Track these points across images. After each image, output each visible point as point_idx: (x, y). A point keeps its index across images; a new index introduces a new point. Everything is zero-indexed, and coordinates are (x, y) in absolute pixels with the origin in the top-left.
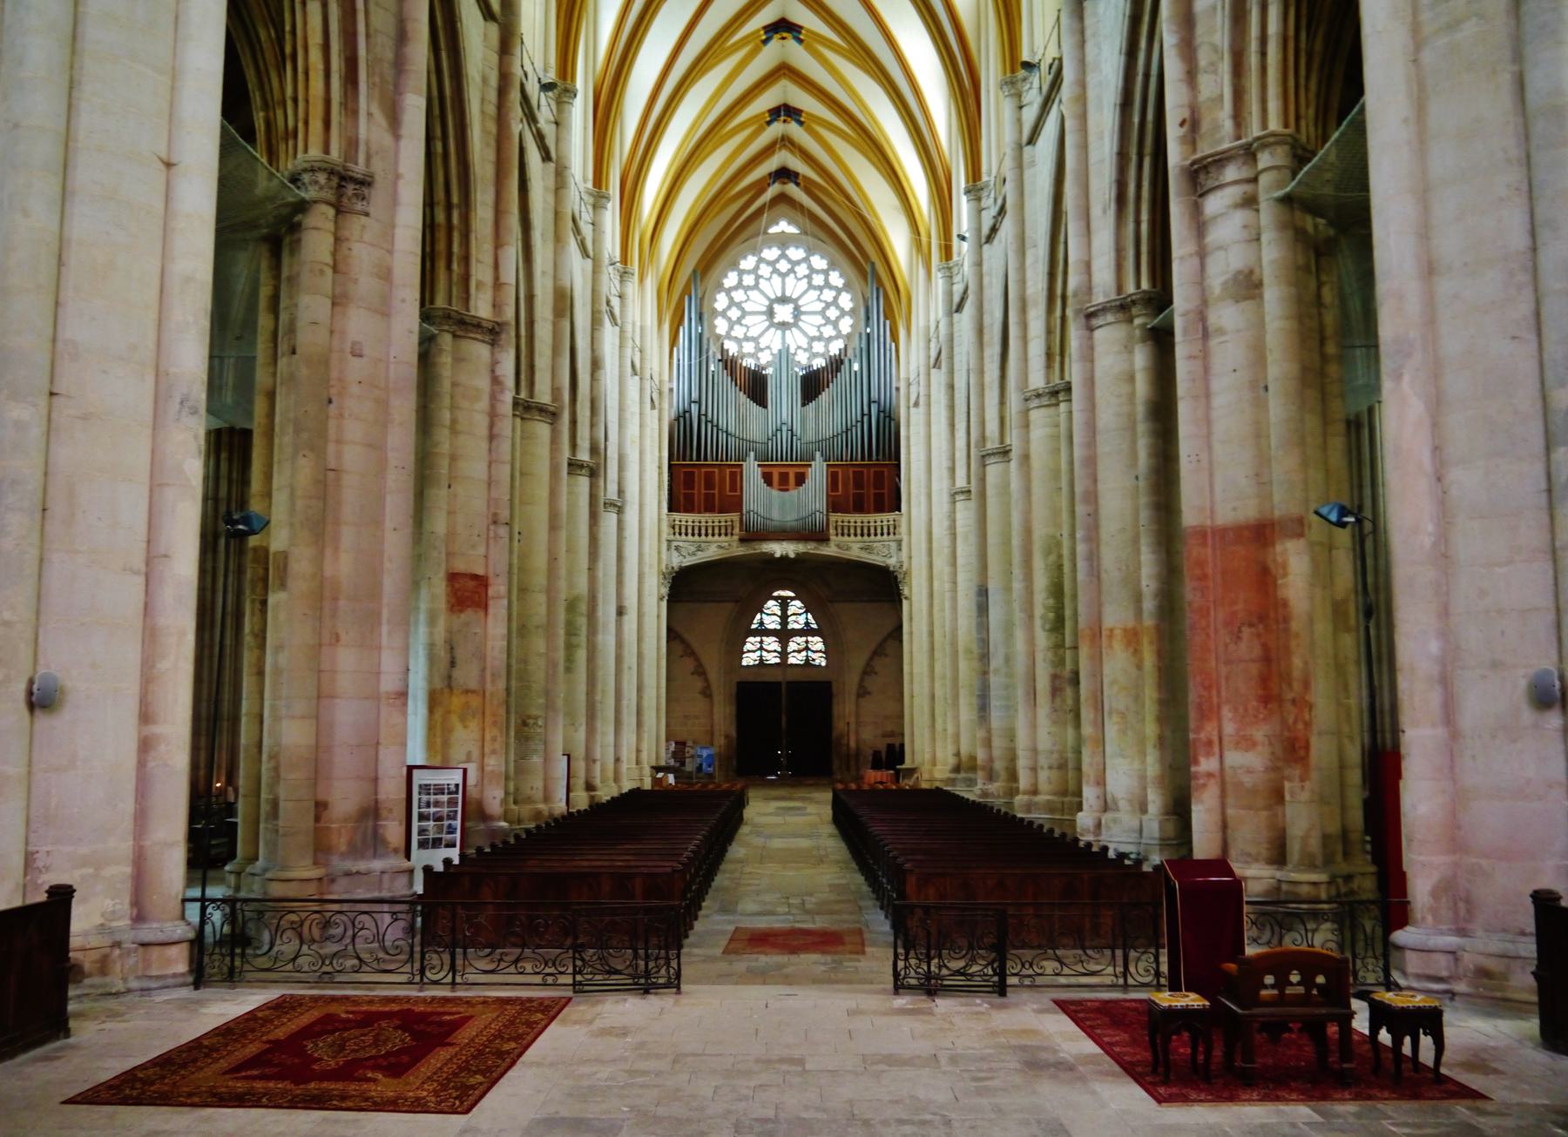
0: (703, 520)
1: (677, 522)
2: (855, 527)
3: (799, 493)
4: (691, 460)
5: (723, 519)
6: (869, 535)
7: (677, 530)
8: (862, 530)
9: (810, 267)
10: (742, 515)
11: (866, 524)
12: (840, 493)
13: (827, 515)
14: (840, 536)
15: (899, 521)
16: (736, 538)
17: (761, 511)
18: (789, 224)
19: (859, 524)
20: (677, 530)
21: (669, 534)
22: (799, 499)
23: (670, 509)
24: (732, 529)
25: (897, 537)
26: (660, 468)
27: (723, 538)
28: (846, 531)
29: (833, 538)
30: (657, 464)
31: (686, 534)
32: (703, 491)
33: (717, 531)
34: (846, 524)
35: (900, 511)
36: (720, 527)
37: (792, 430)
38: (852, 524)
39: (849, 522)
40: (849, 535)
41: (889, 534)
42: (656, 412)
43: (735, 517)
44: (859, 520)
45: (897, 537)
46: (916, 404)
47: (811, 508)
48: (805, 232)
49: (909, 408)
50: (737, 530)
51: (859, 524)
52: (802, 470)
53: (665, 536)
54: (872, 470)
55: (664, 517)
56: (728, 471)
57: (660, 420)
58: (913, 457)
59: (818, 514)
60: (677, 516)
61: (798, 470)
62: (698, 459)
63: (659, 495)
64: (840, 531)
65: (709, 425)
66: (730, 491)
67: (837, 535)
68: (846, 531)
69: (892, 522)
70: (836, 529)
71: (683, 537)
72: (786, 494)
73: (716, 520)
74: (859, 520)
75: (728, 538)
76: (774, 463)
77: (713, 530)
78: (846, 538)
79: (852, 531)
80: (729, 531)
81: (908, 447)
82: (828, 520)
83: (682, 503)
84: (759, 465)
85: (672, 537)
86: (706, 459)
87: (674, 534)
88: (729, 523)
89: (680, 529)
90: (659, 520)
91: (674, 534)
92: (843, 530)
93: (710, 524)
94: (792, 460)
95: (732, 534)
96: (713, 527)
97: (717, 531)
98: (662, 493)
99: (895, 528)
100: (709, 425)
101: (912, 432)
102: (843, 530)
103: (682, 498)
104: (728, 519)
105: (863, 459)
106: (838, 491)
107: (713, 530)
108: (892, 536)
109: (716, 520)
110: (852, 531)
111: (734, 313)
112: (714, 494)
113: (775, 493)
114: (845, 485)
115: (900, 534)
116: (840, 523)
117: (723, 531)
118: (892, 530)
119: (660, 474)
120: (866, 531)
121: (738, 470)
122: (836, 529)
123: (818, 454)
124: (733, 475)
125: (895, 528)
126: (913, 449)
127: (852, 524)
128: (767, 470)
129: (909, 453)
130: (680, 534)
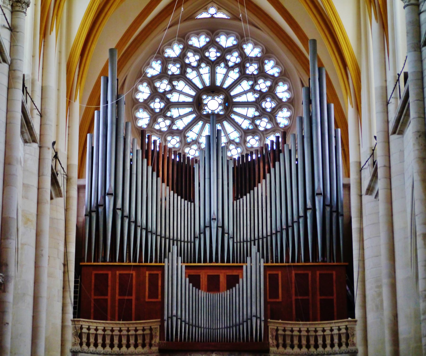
0: (116, 328)
1: (85, 330)
2: (300, 337)
3: (231, 295)
4: (105, 261)
5: (140, 327)
6: (316, 346)
7: (84, 340)
8: (308, 340)
9: (242, 55)
10: (163, 321)
11: (312, 333)
12: (280, 299)
13: (266, 322)
14: (281, 349)
15: (353, 329)
16: (155, 349)
17: (185, 316)
18: (219, 9)
19: (304, 333)
20: (84, 340)
21: (74, 344)
22: (231, 302)
23: (75, 315)
24: (151, 339)
25: (350, 348)
26: (65, 265)
27: (140, 349)
28: (288, 342)
29: (273, 349)
30: (62, 261)
31: (96, 345)
32: (117, 297)
33: (132, 341)
34: (288, 333)
35: (353, 316)
36: (136, 336)
37: (223, 227)
38: (296, 333)
39: (292, 331)
40: (292, 347)
41: (340, 345)
42: (61, 201)
43: (154, 323)
44: (304, 329)
45: (350, 348)
46: (370, 190)
47: (246, 312)
48: (235, 18)
49: (361, 196)
50: (157, 340)
51: (304, 333)
52: (235, 273)
53: (69, 346)
54: (318, 273)
55: (69, 323)
56: (147, 273)
57: (67, 210)
58: (367, 253)
59: (254, 319)
60: (85, 323)
61: (230, 273)
62: (113, 259)
63: (64, 297)
64: (281, 341)
65: (126, 221)
66: (150, 297)
67: (278, 346)
68: (288, 342)
69: (343, 331)
70: (277, 339)
71: (92, 348)
72: (216, 296)
73: (132, 328)
74: (304, 329)
75: (146, 349)
76: (202, 264)
77: (128, 340)
78: (289, 350)
79: (296, 342)
80: (147, 341)
81: (361, 240)
82: (266, 327)
83: (92, 305)
84: (186, 266)
85: (78, 348)
86: (121, 259)
87: (81, 344)
88: (147, 332)
89: (88, 339)
90: (63, 327)
91: (81, 344)
92: (284, 340)
93: (124, 332)
94: (223, 261)
95: (151, 345)
96: (128, 337)
97: (132, 341)
98: (67, 294)
99: (347, 337)
100: (126, 221)
101: (365, 224)
102: (284, 340)
103: (92, 301)
104: (147, 326)
105: (307, 259)
106: (278, 297)
107: (128, 340)
108: (344, 347)
109: (132, 328)
110: (296, 342)
111: (157, 105)
112: (131, 300)
113: (203, 294)
114: (286, 289)
115: (354, 344)
116: (280, 332)
117: (140, 341)
118: (344, 339)
119: (65, 272)
120: (312, 342)
121: (159, 273)
122: (277, 339)
123: (254, 249)
124: (154, 279)
125: (347, 337)
126: (367, 243)
127: (296, 333)
128: (193, 272)
129: (362, 248)
130: (88, 345)
